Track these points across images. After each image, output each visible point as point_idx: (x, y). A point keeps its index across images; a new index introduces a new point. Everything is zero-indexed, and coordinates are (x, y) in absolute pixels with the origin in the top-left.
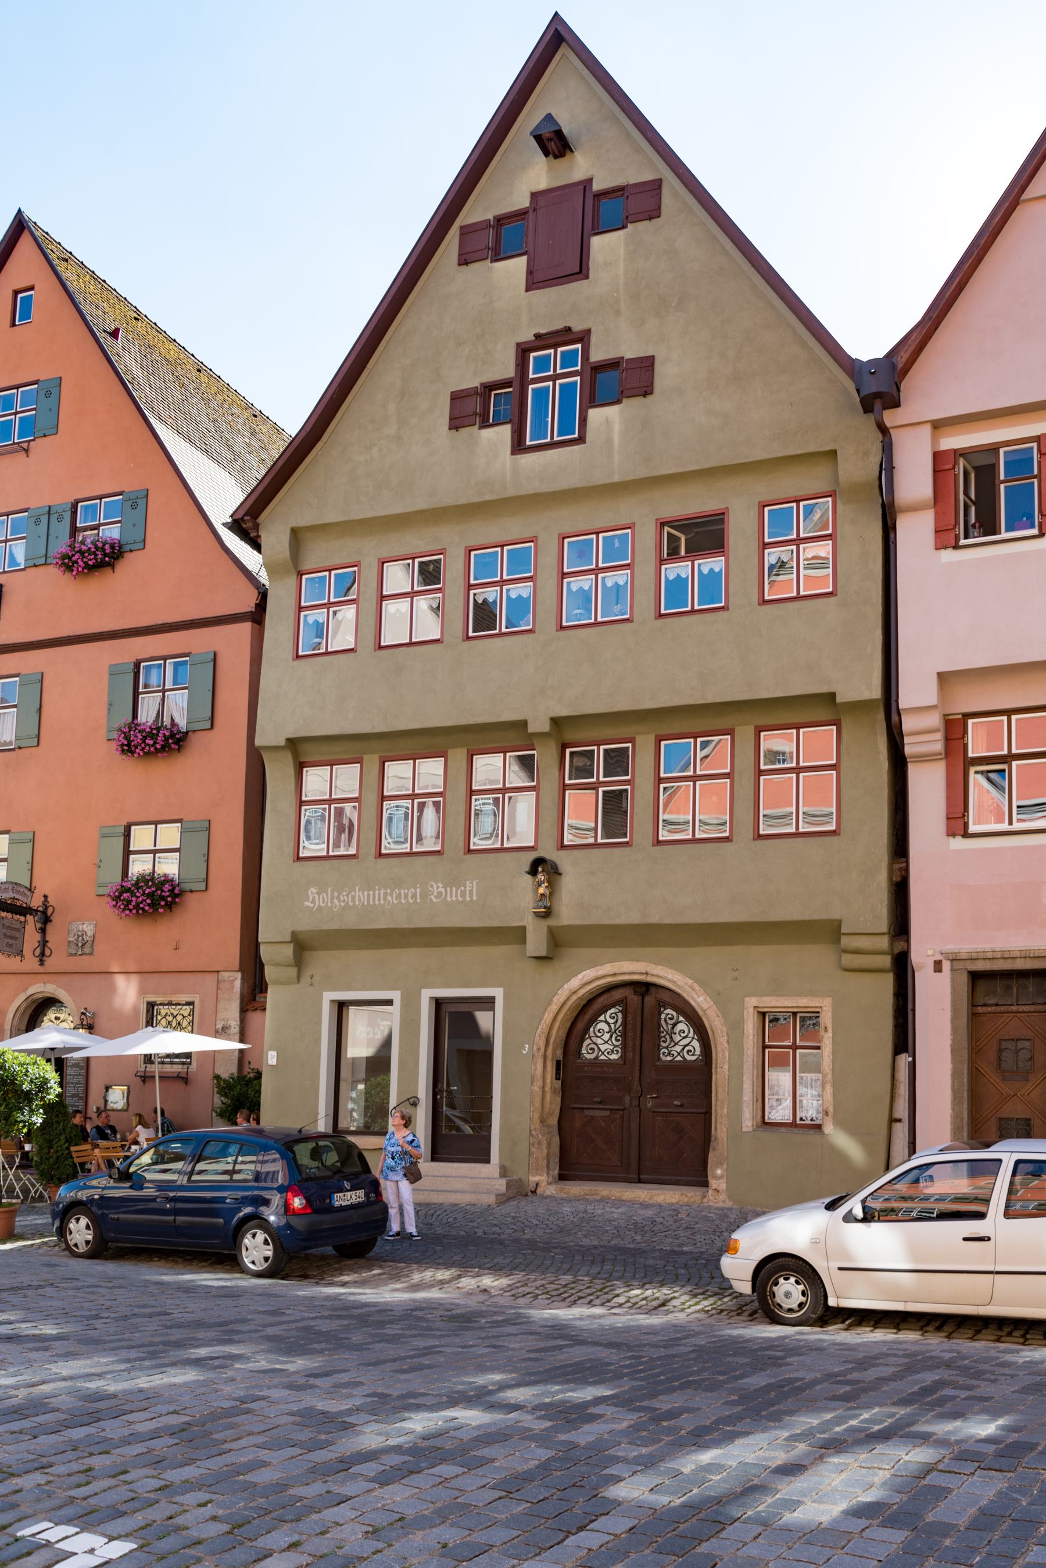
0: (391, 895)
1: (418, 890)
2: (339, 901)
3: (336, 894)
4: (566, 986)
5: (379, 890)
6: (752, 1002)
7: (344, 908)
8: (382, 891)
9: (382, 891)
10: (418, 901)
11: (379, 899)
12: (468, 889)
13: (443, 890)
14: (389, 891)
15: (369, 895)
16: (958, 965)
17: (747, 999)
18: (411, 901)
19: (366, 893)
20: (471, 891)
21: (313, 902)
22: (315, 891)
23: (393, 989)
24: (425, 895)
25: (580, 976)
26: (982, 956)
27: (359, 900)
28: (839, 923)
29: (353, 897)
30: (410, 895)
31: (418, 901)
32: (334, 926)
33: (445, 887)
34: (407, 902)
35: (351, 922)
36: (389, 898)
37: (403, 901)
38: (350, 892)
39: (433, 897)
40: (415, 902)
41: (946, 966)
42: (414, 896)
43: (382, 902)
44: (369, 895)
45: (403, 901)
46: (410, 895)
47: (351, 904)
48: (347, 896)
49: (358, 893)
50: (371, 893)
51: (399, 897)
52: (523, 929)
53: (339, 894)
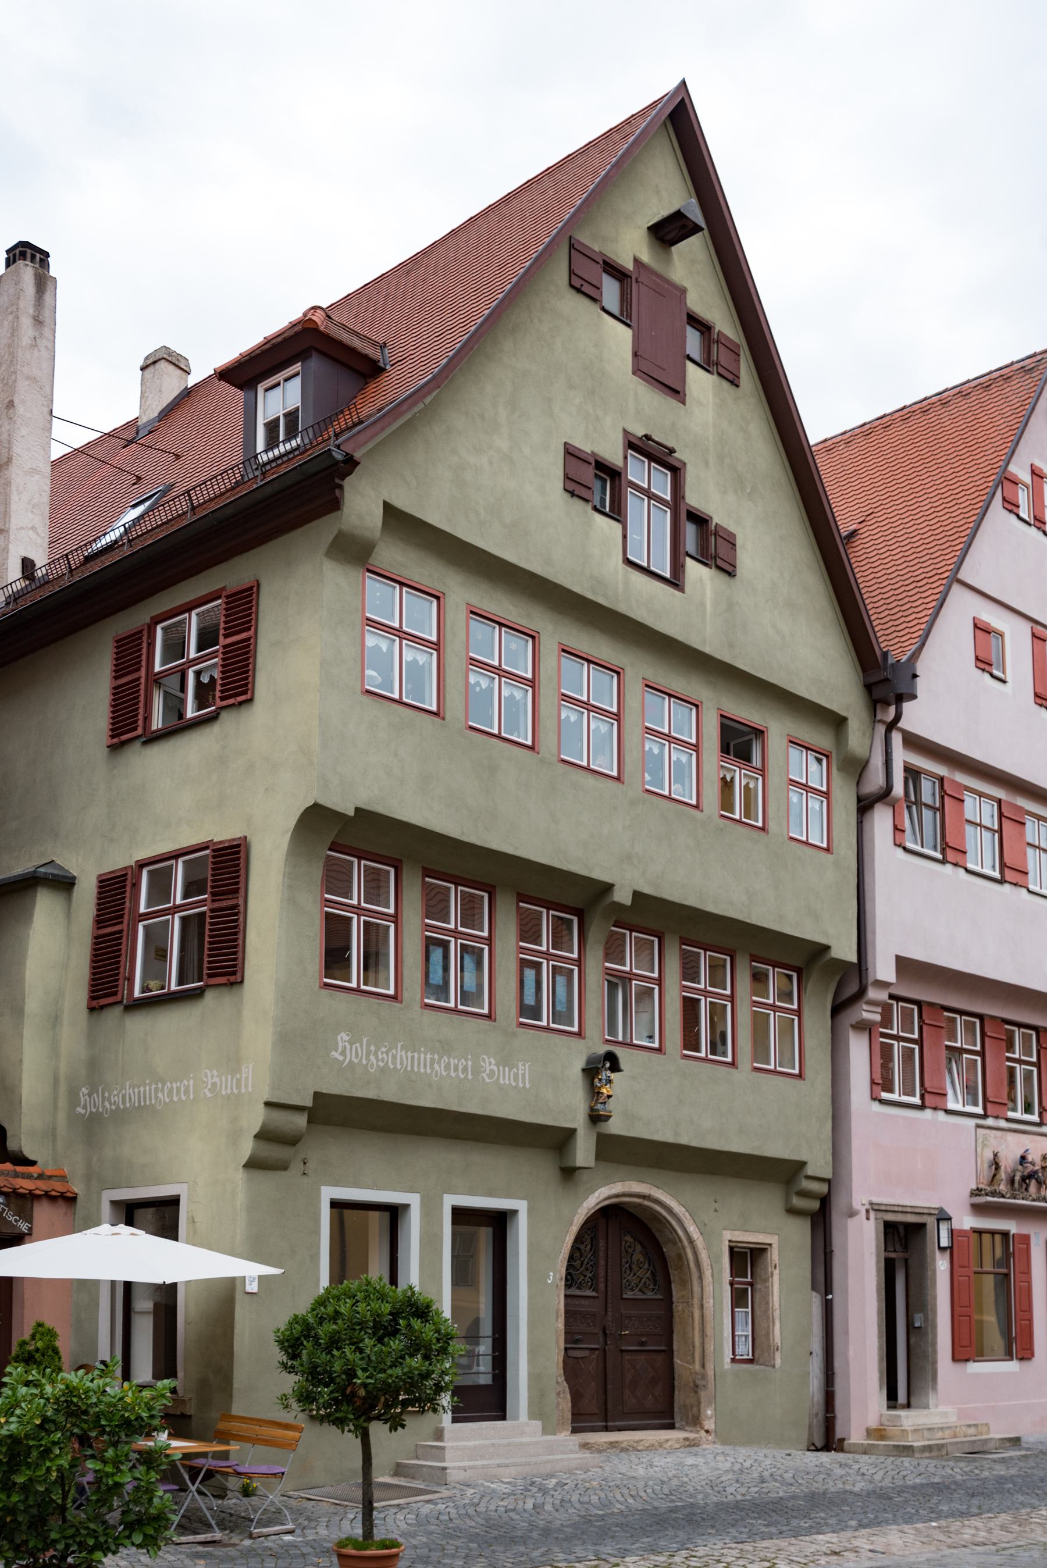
0: (439, 1063)
1: (470, 1063)
2: (377, 1058)
3: (373, 1048)
4: (585, 1204)
5: (426, 1054)
6: (728, 1235)
7: (383, 1071)
8: (429, 1056)
9: (429, 1056)
10: (470, 1077)
11: (425, 1066)
12: (520, 1072)
13: (495, 1068)
14: (436, 1057)
15: (413, 1057)
16: (880, 1215)
17: (724, 1232)
18: (462, 1076)
19: (409, 1054)
20: (524, 1075)
21: (343, 1053)
22: (346, 1038)
23: (411, 1190)
24: (477, 1072)
25: (596, 1194)
26: (892, 1208)
27: (402, 1064)
28: (803, 1164)
29: (394, 1057)
30: (460, 1067)
31: (470, 1077)
32: (371, 1094)
33: (498, 1065)
34: (457, 1076)
35: (390, 1093)
36: (436, 1066)
37: (453, 1074)
38: (390, 1049)
39: (484, 1075)
40: (466, 1077)
41: (872, 1214)
42: (465, 1070)
43: (429, 1071)
44: (413, 1057)
45: (453, 1074)
46: (460, 1067)
47: (392, 1067)
48: (387, 1053)
49: (400, 1054)
50: (416, 1054)
51: (447, 1067)
52: (571, 1133)
53: (378, 1049)
